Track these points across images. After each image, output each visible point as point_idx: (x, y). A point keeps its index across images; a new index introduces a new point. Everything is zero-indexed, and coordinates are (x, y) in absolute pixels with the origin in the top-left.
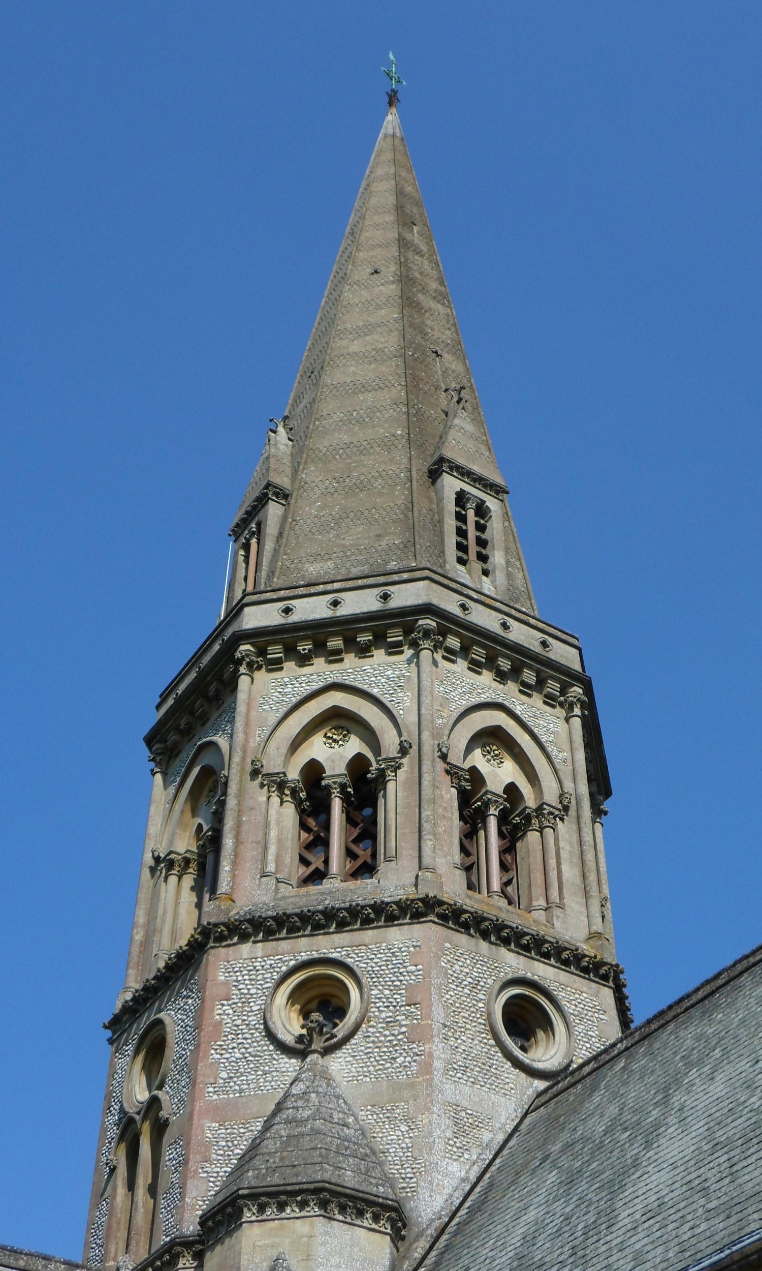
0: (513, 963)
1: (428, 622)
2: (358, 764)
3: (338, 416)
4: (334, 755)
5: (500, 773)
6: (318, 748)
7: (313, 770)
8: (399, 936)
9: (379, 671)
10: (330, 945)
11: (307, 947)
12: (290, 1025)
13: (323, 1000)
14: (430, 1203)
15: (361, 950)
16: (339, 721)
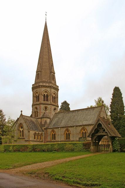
0: (54, 107)
1: (52, 87)
2: (47, 95)
3: (44, 65)
4: (46, 94)
5: (54, 95)
6: (45, 93)
7: (44, 95)
8: (50, 106)
9: (48, 89)
10: (47, 106)
11: (45, 105)
12: (44, 109)
13: (46, 108)
14: (51, 118)
15: (49, 106)
16: (46, 92)
